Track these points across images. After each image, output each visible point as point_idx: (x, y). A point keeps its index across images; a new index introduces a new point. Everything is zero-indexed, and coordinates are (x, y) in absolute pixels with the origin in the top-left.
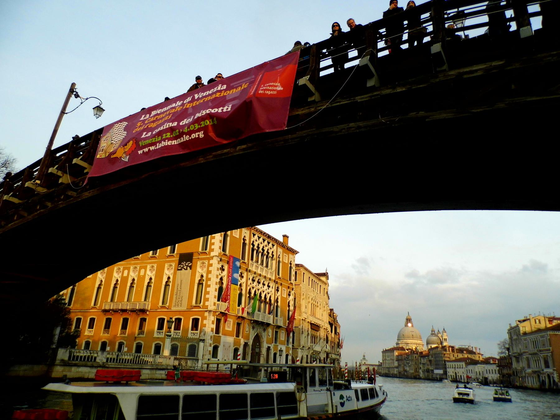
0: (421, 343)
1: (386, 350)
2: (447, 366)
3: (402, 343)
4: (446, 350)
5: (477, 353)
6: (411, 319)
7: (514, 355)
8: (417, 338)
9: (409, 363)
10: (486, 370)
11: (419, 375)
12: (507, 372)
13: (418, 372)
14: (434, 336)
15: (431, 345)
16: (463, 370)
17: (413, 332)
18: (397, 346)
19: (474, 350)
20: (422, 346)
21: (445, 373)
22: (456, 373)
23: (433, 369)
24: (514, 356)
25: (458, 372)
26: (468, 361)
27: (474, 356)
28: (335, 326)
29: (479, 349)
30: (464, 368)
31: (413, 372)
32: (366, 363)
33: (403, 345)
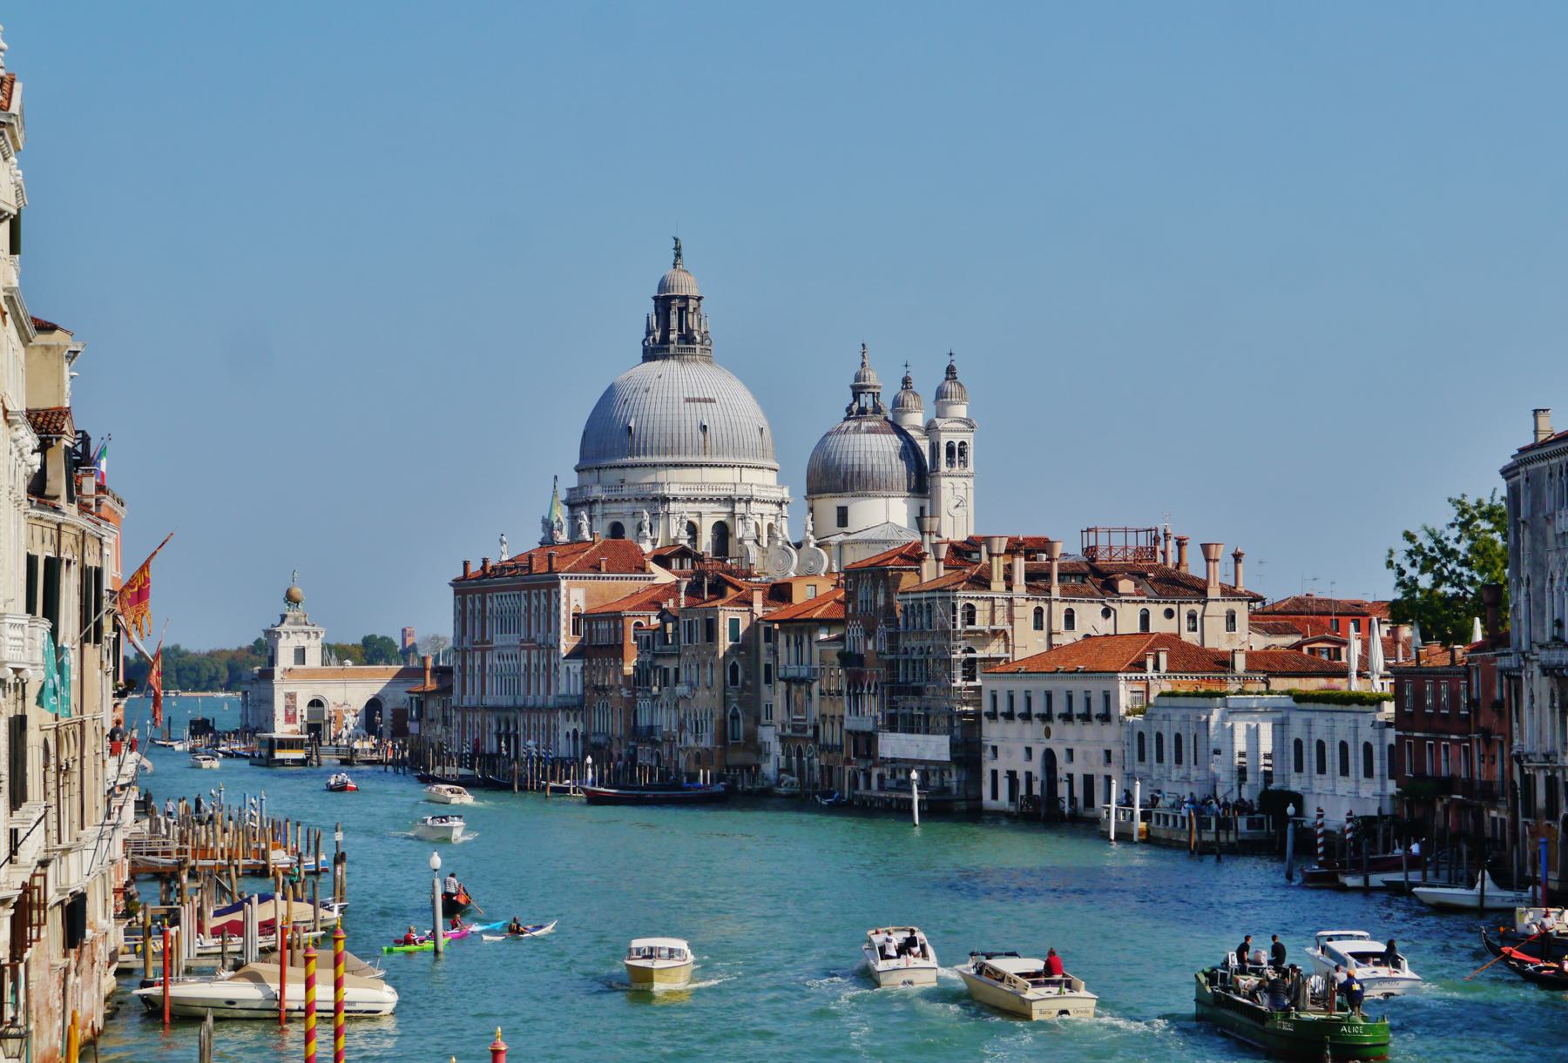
0: (764, 495)
2: (987, 707)
3: (614, 495)
4: (982, 581)
5: (1214, 592)
6: (699, 299)
7: (1544, 656)
8: (735, 451)
9: (677, 671)
10: (1298, 743)
11: (753, 771)
12: (1463, 775)
13: (752, 738)
14: (870, 431)
15: (842, 502)
16: (1109, 735)
17: (711, 401)
18: (574, 519)
19: (1194, 567)
20: (774, 509)
21: (968, 753)
22: (1049, 756)
23: (868, 726)
24: (1546, 670)
25: (1070, 752)
26: (1150, 662)
27: (1192, 617)
28: (85, 572)
29: (1237, 557)
31: (707, 742)
33: (626, 508)
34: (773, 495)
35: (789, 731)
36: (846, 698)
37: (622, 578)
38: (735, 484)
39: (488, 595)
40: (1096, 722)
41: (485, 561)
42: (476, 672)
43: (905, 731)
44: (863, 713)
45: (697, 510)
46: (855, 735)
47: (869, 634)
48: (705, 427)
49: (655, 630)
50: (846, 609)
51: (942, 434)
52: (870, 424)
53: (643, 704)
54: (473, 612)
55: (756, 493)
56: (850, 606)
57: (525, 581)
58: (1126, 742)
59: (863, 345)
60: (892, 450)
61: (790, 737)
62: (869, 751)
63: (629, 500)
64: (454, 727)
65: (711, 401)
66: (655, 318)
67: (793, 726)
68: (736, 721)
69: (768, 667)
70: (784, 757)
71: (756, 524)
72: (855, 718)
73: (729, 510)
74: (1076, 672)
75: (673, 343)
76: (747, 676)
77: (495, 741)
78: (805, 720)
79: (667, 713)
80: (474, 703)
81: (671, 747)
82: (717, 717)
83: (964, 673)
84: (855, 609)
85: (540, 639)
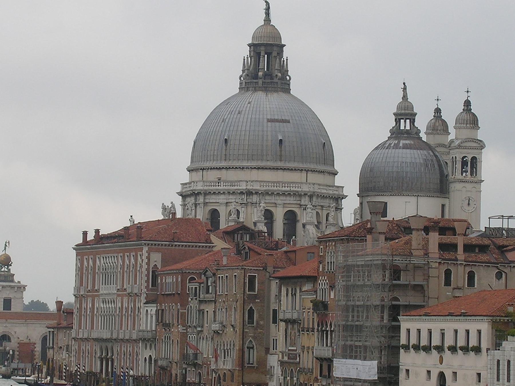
1: (100, 238)
2: (403, 341)
14: (405, 147)
17: (289, 122)
18: (184, 205)
23: (326, 353)
25: (455, 373)
30: (488, 350)
31: (229, 366)
32: (16, 308)
33: (222, 199)
34: (331, 192)
35: (286, 359)
36: (316, 333)
37: (189, 246)
38: (302, 183)
39: (97, 256)
40: (472, 354)
41: (97, 231)
42: (88, 313)
43: (351, 357)
44: (327, 345)
45: (273, 201)
46: (321, 360)
47: (332, 287)
48: (281, 140)
49: (200, 283)
50: (319, 267)
51: (460, 150)
52: (407, 142)
53: (192, 338)
54: (87, 269)
55: (316, 189)
56: (321, 266)
57: (121, 246)
58: (489, 366)
59: (404, 84)
60: (422, 162)
61: (286, 362)
62: (329, 374)
63: (224, 192)
64: (73, 353)
65: (289, 122)
66: (249, 58)
67: (289, 354)
68: (251, 350)
69: (275, 311)
70: (283, 378)
71: (317, 213)
72: (320, 347)
73: (299, 202)
74: (460, 316)
75: (261, 78)
76: (261, 317)
77: (99, 363)
78: (296, 350)
79: (206, 343)
80: (86, 336)
81: (208, 368)
82: (238, 348)
83: (390, 316)
84: (324, 268)
85: (129, 291)
